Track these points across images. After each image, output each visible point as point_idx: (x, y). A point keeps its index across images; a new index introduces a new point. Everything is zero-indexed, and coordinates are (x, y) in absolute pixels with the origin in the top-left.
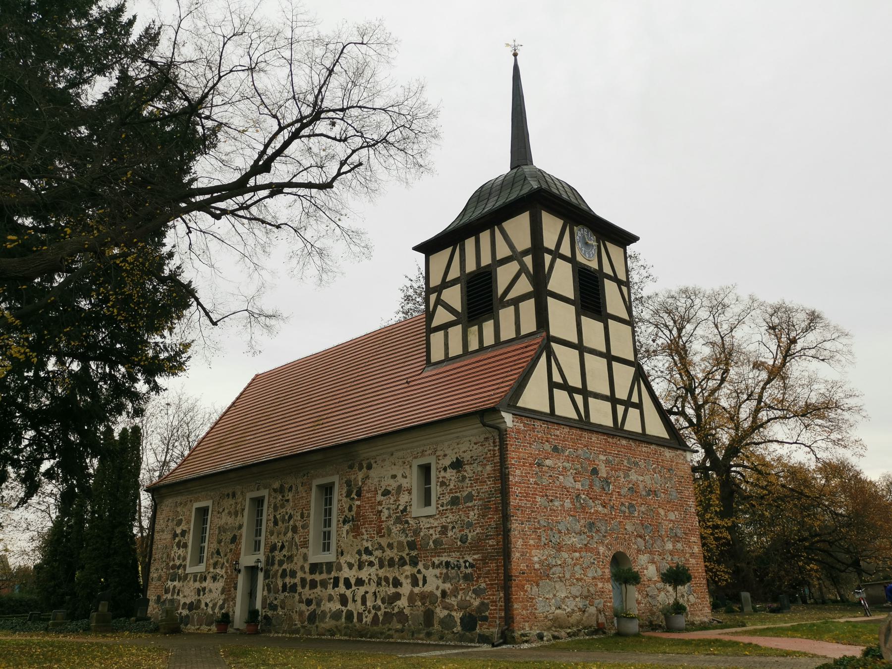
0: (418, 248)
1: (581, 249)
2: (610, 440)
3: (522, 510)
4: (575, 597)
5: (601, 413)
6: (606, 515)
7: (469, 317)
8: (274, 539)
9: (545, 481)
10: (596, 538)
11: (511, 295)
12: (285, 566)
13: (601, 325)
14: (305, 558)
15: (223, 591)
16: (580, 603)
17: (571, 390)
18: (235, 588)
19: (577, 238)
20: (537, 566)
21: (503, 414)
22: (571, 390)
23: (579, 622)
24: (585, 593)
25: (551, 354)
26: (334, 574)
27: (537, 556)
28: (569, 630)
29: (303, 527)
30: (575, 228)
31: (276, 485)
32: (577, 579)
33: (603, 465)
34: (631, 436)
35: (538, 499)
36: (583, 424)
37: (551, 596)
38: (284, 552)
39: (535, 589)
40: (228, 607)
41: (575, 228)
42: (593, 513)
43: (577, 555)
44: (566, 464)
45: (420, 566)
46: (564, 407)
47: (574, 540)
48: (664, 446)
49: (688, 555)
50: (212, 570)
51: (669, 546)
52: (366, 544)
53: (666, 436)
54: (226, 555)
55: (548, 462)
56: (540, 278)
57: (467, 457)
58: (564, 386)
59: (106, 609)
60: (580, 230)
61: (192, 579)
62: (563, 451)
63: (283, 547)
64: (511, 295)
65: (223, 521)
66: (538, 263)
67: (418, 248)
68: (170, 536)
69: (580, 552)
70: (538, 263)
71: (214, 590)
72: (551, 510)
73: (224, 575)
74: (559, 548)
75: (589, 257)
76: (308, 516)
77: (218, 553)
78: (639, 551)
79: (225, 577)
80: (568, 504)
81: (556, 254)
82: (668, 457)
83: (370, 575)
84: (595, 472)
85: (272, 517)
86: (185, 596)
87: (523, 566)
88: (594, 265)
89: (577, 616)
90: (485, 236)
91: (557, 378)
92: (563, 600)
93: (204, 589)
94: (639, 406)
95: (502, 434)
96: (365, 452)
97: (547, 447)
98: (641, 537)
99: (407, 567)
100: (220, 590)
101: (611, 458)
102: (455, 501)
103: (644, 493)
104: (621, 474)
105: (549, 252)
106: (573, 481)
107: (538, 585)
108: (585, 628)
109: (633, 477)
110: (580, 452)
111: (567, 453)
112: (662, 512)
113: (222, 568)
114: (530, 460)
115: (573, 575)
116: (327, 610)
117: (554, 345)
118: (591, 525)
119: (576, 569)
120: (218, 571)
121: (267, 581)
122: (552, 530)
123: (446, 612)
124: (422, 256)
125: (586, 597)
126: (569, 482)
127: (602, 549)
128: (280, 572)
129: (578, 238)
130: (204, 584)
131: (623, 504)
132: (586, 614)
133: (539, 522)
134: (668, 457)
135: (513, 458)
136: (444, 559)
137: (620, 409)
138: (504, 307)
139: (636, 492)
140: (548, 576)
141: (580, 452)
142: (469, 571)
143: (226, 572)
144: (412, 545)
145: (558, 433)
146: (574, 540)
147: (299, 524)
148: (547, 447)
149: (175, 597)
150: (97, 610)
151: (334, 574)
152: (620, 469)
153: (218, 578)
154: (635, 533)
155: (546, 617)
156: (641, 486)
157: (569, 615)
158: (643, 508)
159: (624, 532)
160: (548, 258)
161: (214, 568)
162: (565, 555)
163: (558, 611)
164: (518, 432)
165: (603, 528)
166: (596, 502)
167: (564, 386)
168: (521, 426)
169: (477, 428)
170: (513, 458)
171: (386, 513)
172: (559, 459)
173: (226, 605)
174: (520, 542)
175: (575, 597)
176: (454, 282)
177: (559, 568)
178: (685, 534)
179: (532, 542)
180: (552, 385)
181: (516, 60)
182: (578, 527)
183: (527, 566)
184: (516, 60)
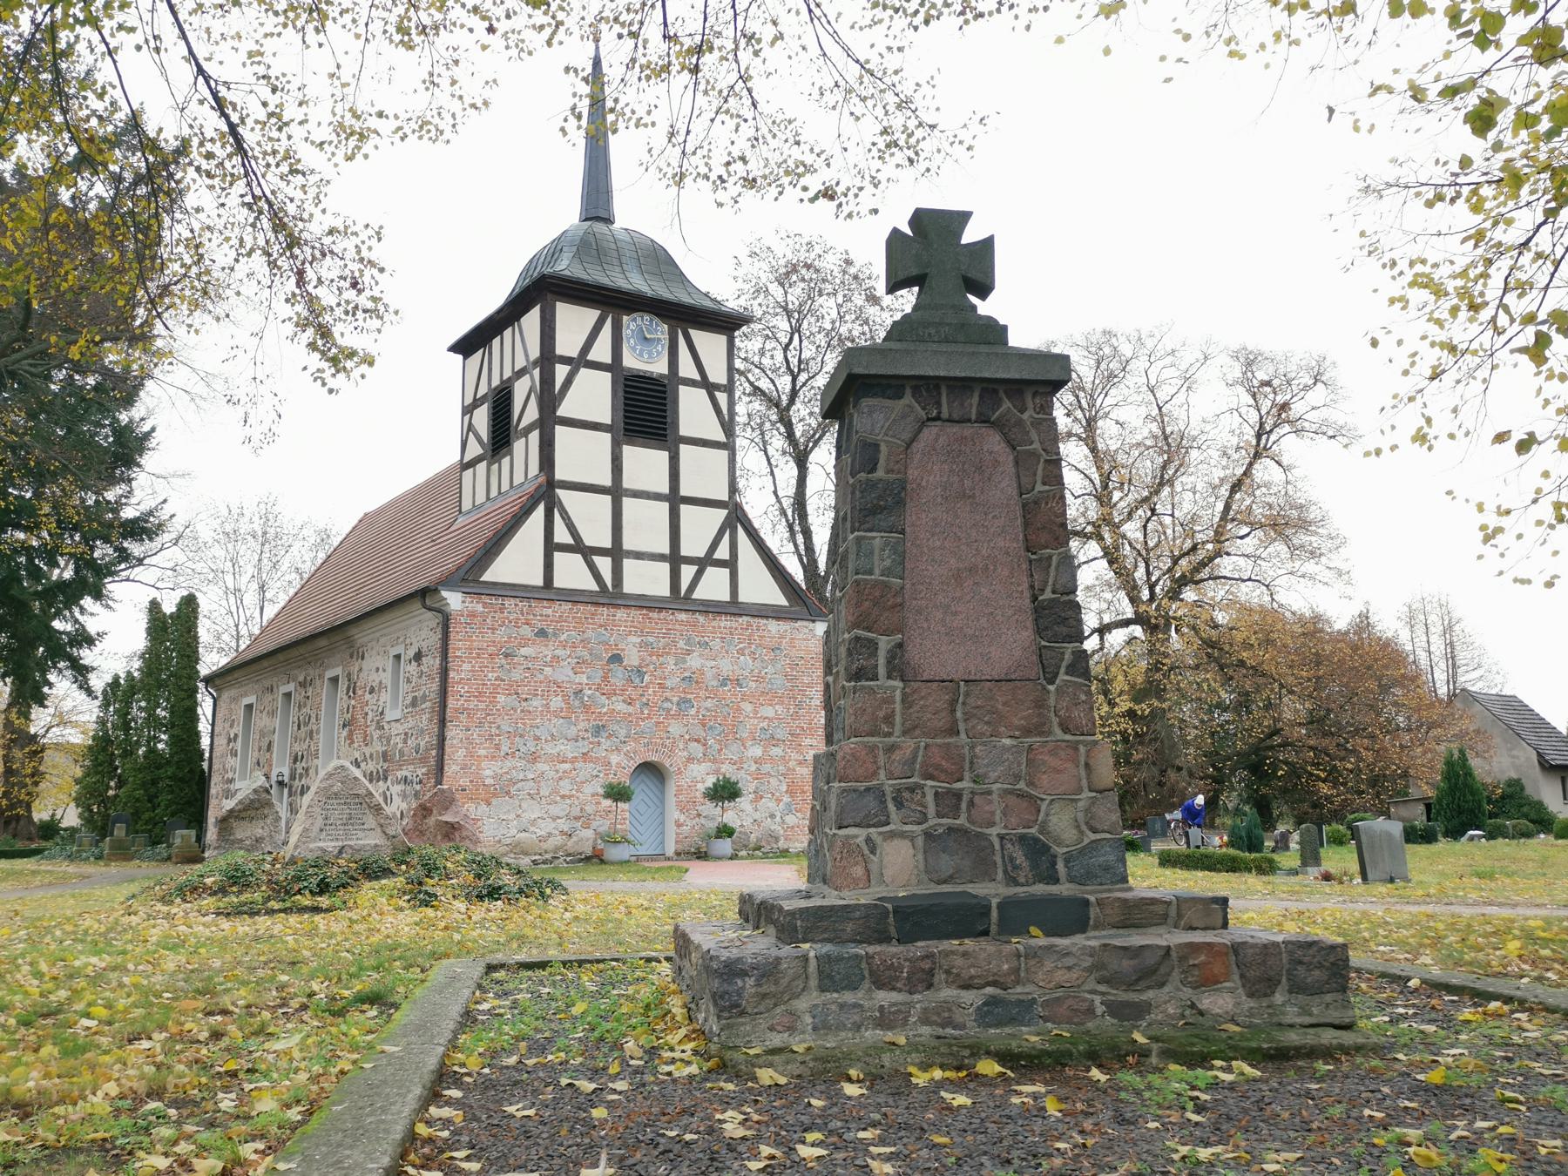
0: (455, 348)
1: (634, 349)
2: (654, 615)
3: (469, 714)
4: (555, 819)
5: (645, 579)
6: (630, 715)
7: (493, 450)
8: (297, 747)
9: (517, 675)
10: (606, 744)
11: (522, 425)
12: (303, 782)
13: (664, 456)
16: (564, 825)
17: (587, 553)
19: (626, 332)
20: (488, 781)
21: (444, 594)
22: (587, 553)
23: (557, 849)
24: (576, 812)
25: (552, 505)
27: (489, 771)
28: (537, 857)
30: (625, 318)
31: (301, 679)
32: (563, 797)
33: (635, 650)
34: (712, 608)
35: (501, 699)
36: (611, 596)
37: (512, 816)
38: (303, 764)
39: (483, 807)
41: (625, 318)
42: (606, 714)
43: (567, 766)
44: (559, 652)
46: (571, 572)
47: (568, 749)
48: (767, 617)
49: (793, 763)
51: (757, 751)
52: (357, 754)
53: (783, 601)
55: (524, 651)
56: (549, 399)
57: (424, 645)
58: (578, 547)
59: (123, 834)
60: (634, 320)
62: (555, 634)
64: (523, 424)
65: (262, 724)
66: (547, 379)
67: (455, 348)
68: (225, 741)
69: (572, 762)
70: (547, 379)
72: (522, 711)
74: (534, 758)
75: (650, 353)
78: (690, 759)
80: (557, 702)
81: (580, 361)
82: (774, 632)
84: (616, 658)
85: (296, 719)
87: (464, 782)
88: (660, 367)
89: (557, 840)
90: (508, 333)
91: (562, 535)
92: (533, 822)
94: (731, 564)
95: (446, 621)
96: (361, 635)
97: (526, 631)
98: (698, 741)
99: (381, 783)
101: (651, 639)
102: (414, 703)
103: (715, 683)
104: (671, 660)
105: (566, 360)
106: (571, 673)
107: (489, 804)
108: (569, 855)
109: (694, 662)
110: (589, 633)
111: (563, 637)
112: (747, 707)
114: (491, 650)
115: (555, 791)
117: (558, 491)
118: (598, 730)
119: (561, 783)
122: (521, 736)
124: (460, 357)
125: (577, 818)
126: (564, 674)
127: (614, 759)
129: (629, 332)
131: (667, 699)
132: (574, 839)
133: (498, 727)
134: (774, 632)
135: (459, 649)
136: (404, 773)
137: (688, 572)
138: (518, 438)
139: (697, 682)
140: (508, 793)
141: (589, 633)
142: (418, 787)
144: (385, 756)
145: (545, 612)
146: (568, 749)
147: (315, 728)
148: (526, 631)
150: (112, 835)
152: (668, 653)
154: (687, 737)
155: (500, 841)
156: (709, 674)
157: (542, 839)
158: (709, 703)
159: (665, 735)
160: (561, 371)
162: (541, 767)
163: (523, 835)
164: (472, 615)
165: (623, 732)
166: (614, 699)
167: (578, 547)
168: (480, 608)
170: (459, 649)
171: (370, 717)
172: (546, 646)
174: (461, 753)
175: (555, 819)
176: (485, 396)
177: (531, 783)
178: (792, 735)
179: (482, 752)
180: (550, 547)
181: (597, 48)
182: (573, 731)
183: (471, 781)
184: (597, 48)
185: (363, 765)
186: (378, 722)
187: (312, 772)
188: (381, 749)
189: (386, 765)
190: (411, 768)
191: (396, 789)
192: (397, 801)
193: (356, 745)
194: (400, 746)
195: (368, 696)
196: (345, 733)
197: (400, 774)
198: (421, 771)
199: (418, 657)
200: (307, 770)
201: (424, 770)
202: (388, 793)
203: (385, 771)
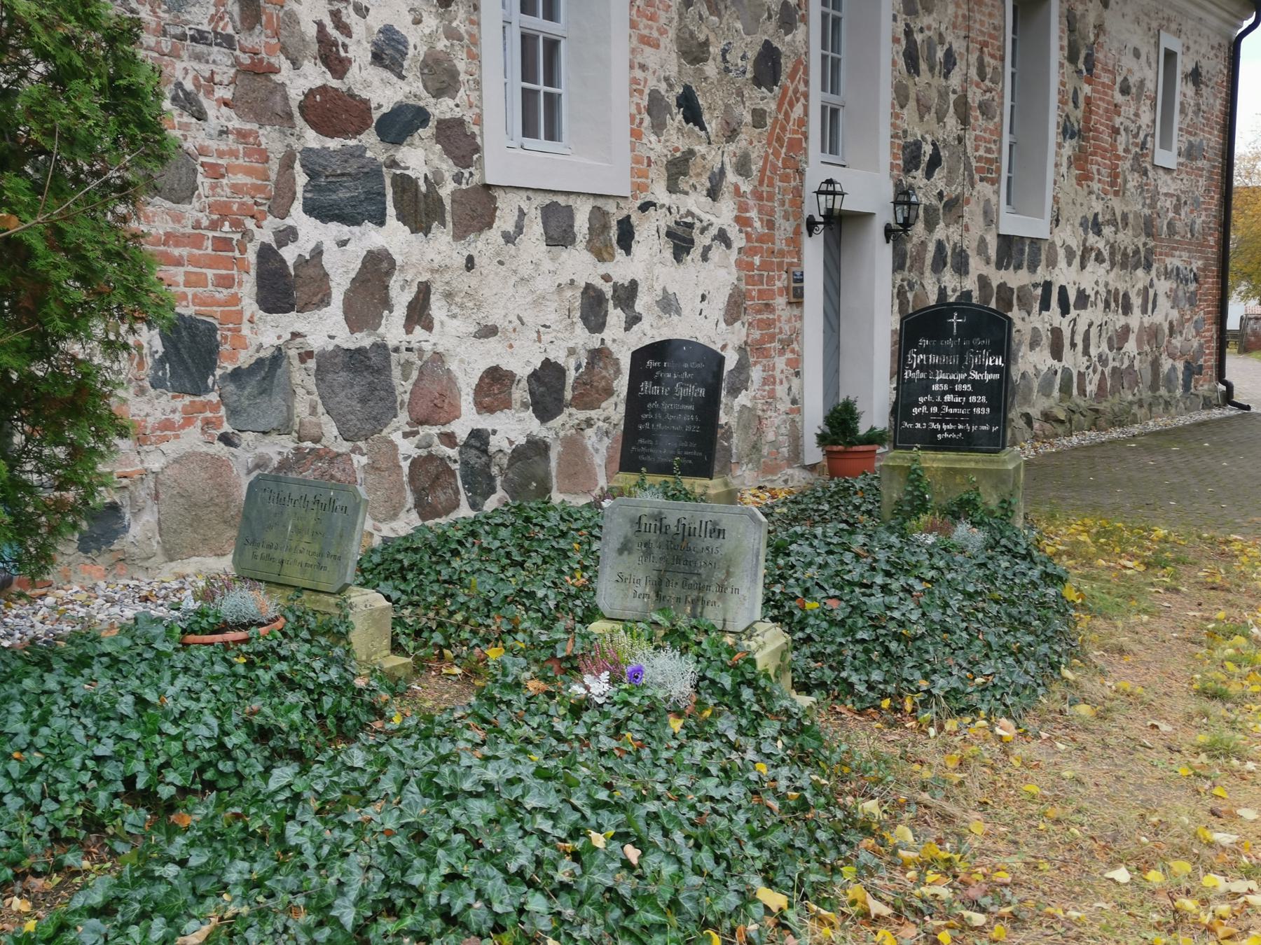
12: (940, 232)
14: (989, 218)
15: (735, 309)
18: (796, 297)
26: (1041, 274)
29: (985, 108)
40: (769, 380)
45: (1153, 272)
50: (660, 193)
52: (1098, 207)
54: (731, 134)
61: (535, 228)
63: (935, 162)
71: (688, 302)
73: (733, 232)
76: (998, 77)
77: (691, 110)
79: (738, 241)
83: (1097, 283)
86: (488, 331)
93: (627, 294)
99: (1140, 272)
100: (719, 301)
113: (713, 193)
116: (1031, 371)
120: (695, 203)
121: (899, 277)
123: (1170, 361)
128: (931, 248)
130: (623, 268)
143: (742, 222)
149: (392, 329)
151: (1041, 274)
153: (701, 241)
161: (672, 188)
169: (1218, 17)
173: (756, 374)
185: (1107, 231)
186: (1137, 157)
187: (972, 212)
188: (1136, 206)
189: (1151, 244)
190: (1185, 255)
191: (1163, 286)
192: (1164, 303)
193: (1096, 186)
194: (1171, 215)
195: (1119, 98)
196: (1069, 148)
197: (1173, 262)
198: (1197, 264)
199: (1195, 76)
200: (953, 206)
201: (1200, 263)
202: (1151, 292)
203: (1150, 252)
